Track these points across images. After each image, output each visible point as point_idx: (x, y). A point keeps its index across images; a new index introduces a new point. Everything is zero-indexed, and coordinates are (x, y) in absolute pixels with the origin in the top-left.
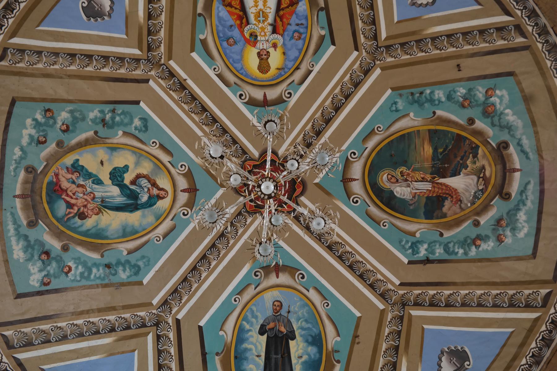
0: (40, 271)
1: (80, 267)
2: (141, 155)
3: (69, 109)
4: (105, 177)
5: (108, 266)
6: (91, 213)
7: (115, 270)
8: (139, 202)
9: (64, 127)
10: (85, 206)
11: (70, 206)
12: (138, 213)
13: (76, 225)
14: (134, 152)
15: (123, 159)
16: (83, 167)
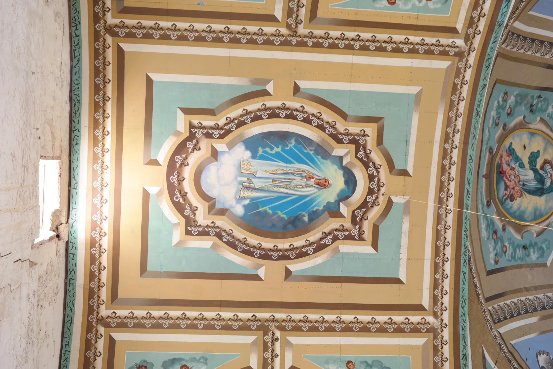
0: (494, 249)
1: (511, 247)
2: (549, 141)
3: (516, 93)
4: (526, 161)
5: (525, 247)
6: (517, 196)
7: (529, 252)
8: (545, 187)
9: (509, 112)
10: (514, 188)
11: (507, 187)
12: (544, 198)
13: (509, 207)
14: (544, 138)
15: (537, 145)
16: (514, 149)
